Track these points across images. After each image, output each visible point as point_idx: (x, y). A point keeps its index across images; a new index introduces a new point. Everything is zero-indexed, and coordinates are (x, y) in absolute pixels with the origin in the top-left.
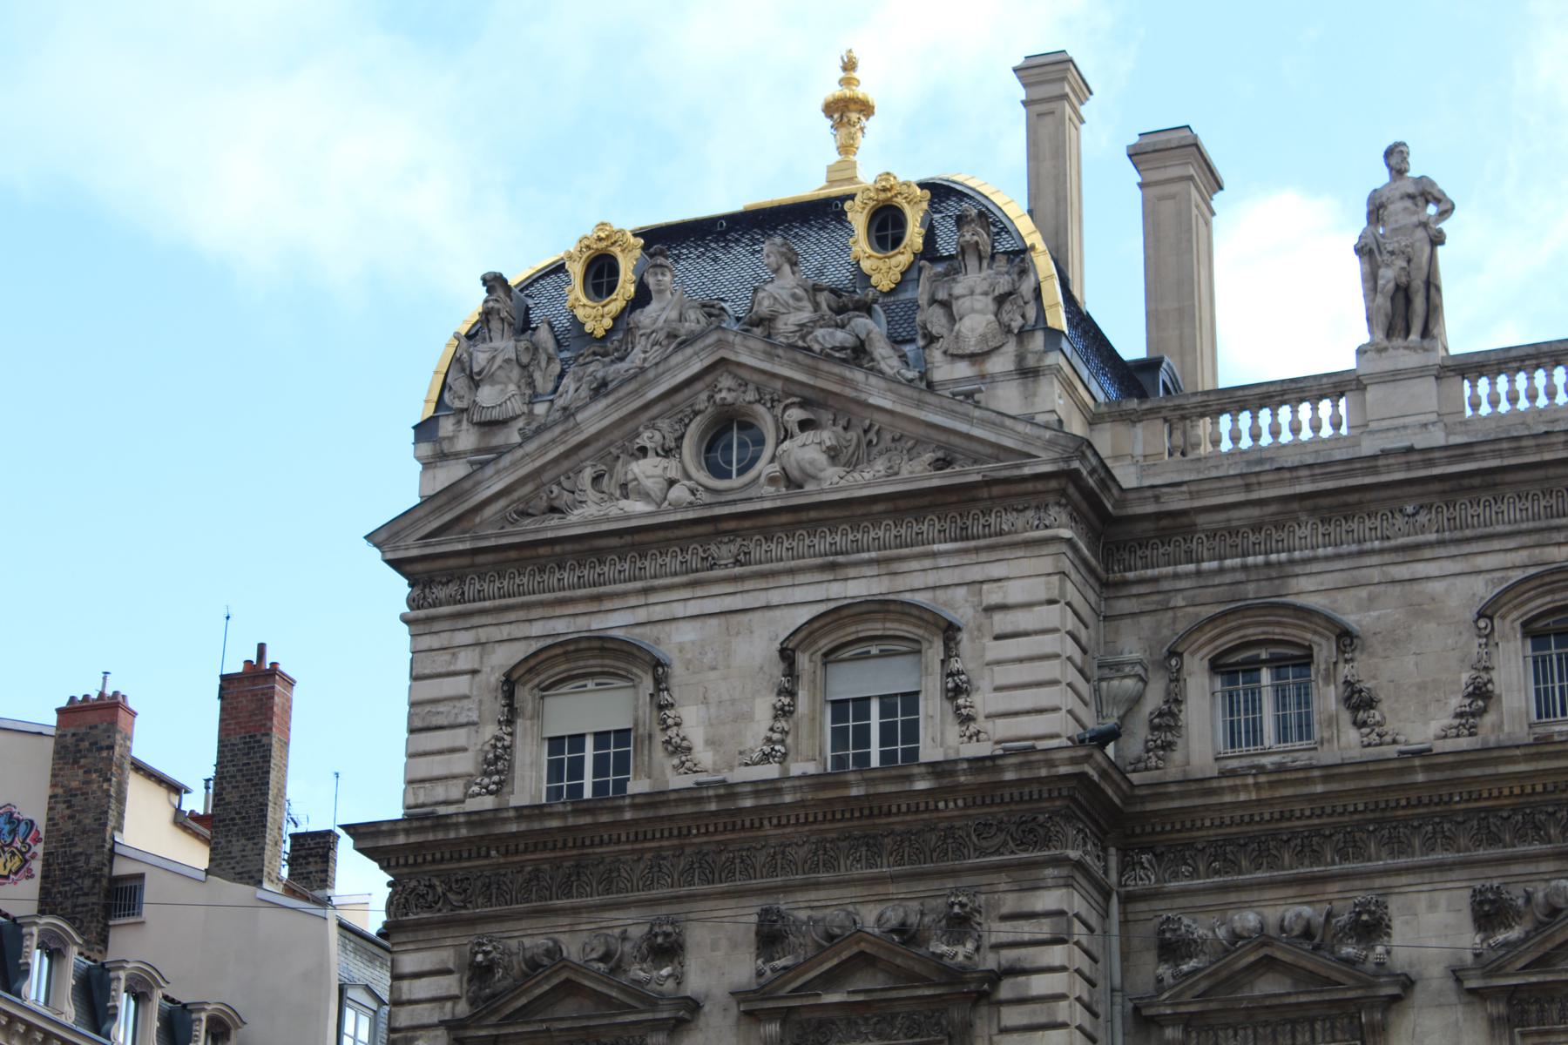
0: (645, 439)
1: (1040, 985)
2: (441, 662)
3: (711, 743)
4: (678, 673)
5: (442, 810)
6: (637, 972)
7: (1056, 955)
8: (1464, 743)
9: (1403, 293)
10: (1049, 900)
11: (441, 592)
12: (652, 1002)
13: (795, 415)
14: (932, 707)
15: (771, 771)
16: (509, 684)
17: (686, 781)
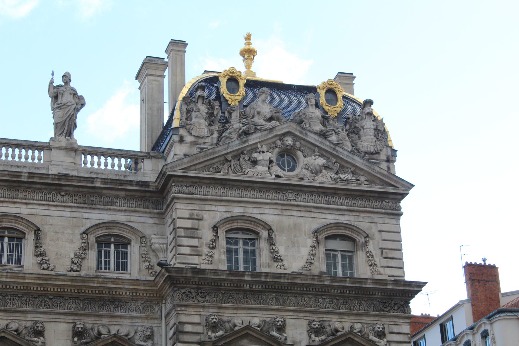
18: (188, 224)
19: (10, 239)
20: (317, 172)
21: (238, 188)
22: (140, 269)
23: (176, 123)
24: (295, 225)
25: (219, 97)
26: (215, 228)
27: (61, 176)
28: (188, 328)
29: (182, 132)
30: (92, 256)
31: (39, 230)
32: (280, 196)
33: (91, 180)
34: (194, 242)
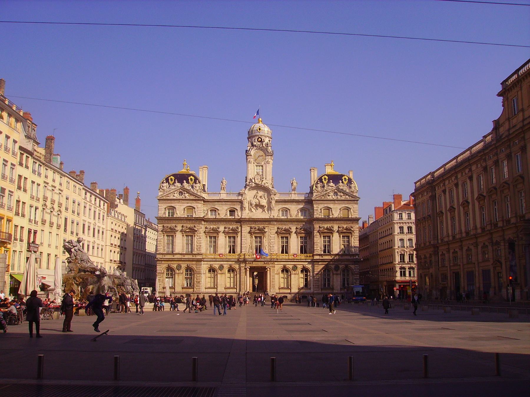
0: (175, 193)
1: (200, 231)
2: (160, 206)
3: (179, 214)
4: (177, 209)
5: (162, 216)
6: (175, 228)
7: (201, 229)
8: (225, 218)
9: (223, 188)
10: (200, 226)
11: (160, 201)
12: (176, 230)
13: (186, 193)
14: (194, 213)
15: (183, 216)
16: (165, 208)
17: (177, 216)
18: (316, 208)
19: (285, 211)
20: (341, 196)
21: (326, 201)
22: (308, 216)
23: (314, 189)
24: (337, 207)
25: (322, 182)
26: (321, 209)
27: (294, 200)
28: (316, 228)
29: (315, 190)
30: (300, 214)
31: (290, 210)
32: (334, 202)
33: (299, 200)
34: (317, 212)
